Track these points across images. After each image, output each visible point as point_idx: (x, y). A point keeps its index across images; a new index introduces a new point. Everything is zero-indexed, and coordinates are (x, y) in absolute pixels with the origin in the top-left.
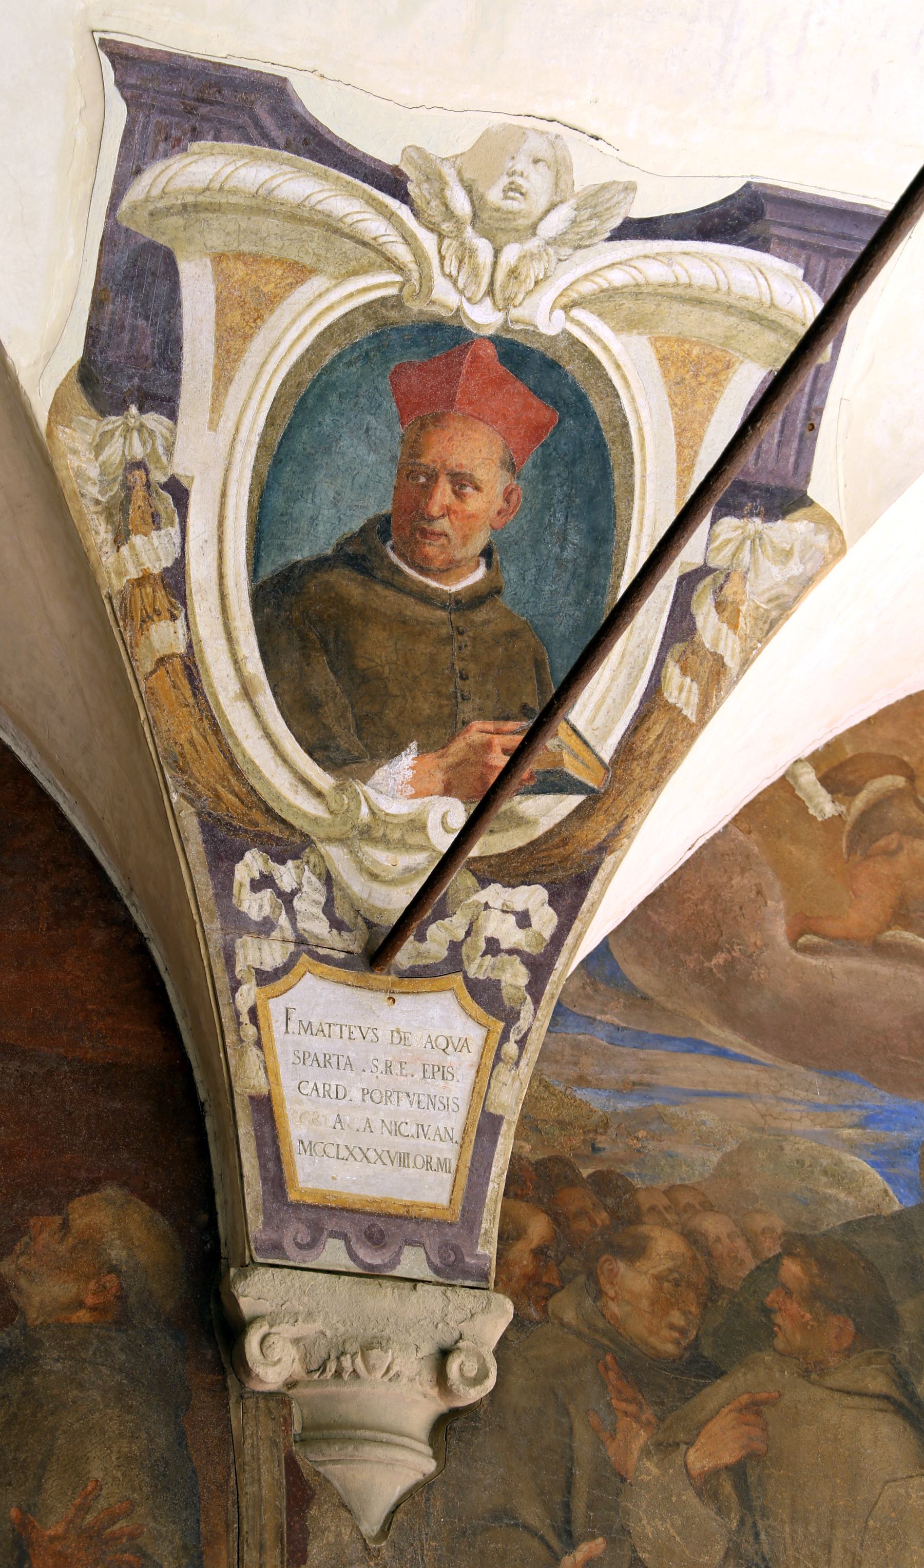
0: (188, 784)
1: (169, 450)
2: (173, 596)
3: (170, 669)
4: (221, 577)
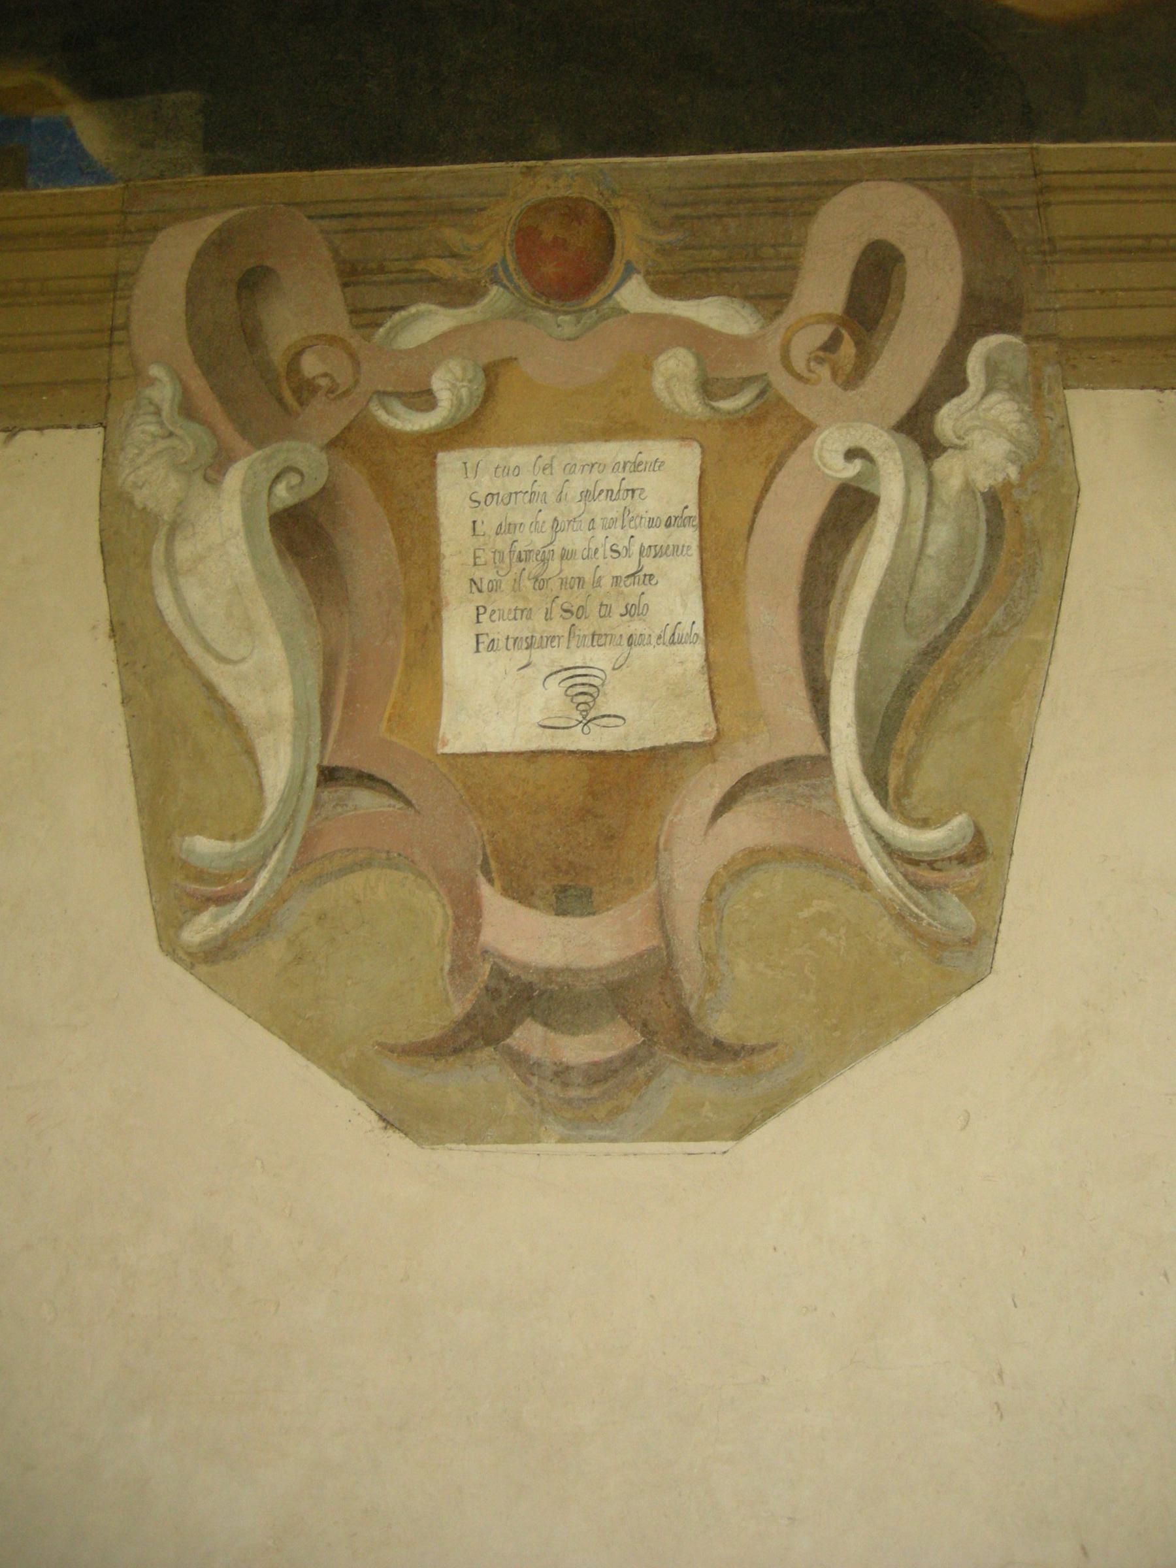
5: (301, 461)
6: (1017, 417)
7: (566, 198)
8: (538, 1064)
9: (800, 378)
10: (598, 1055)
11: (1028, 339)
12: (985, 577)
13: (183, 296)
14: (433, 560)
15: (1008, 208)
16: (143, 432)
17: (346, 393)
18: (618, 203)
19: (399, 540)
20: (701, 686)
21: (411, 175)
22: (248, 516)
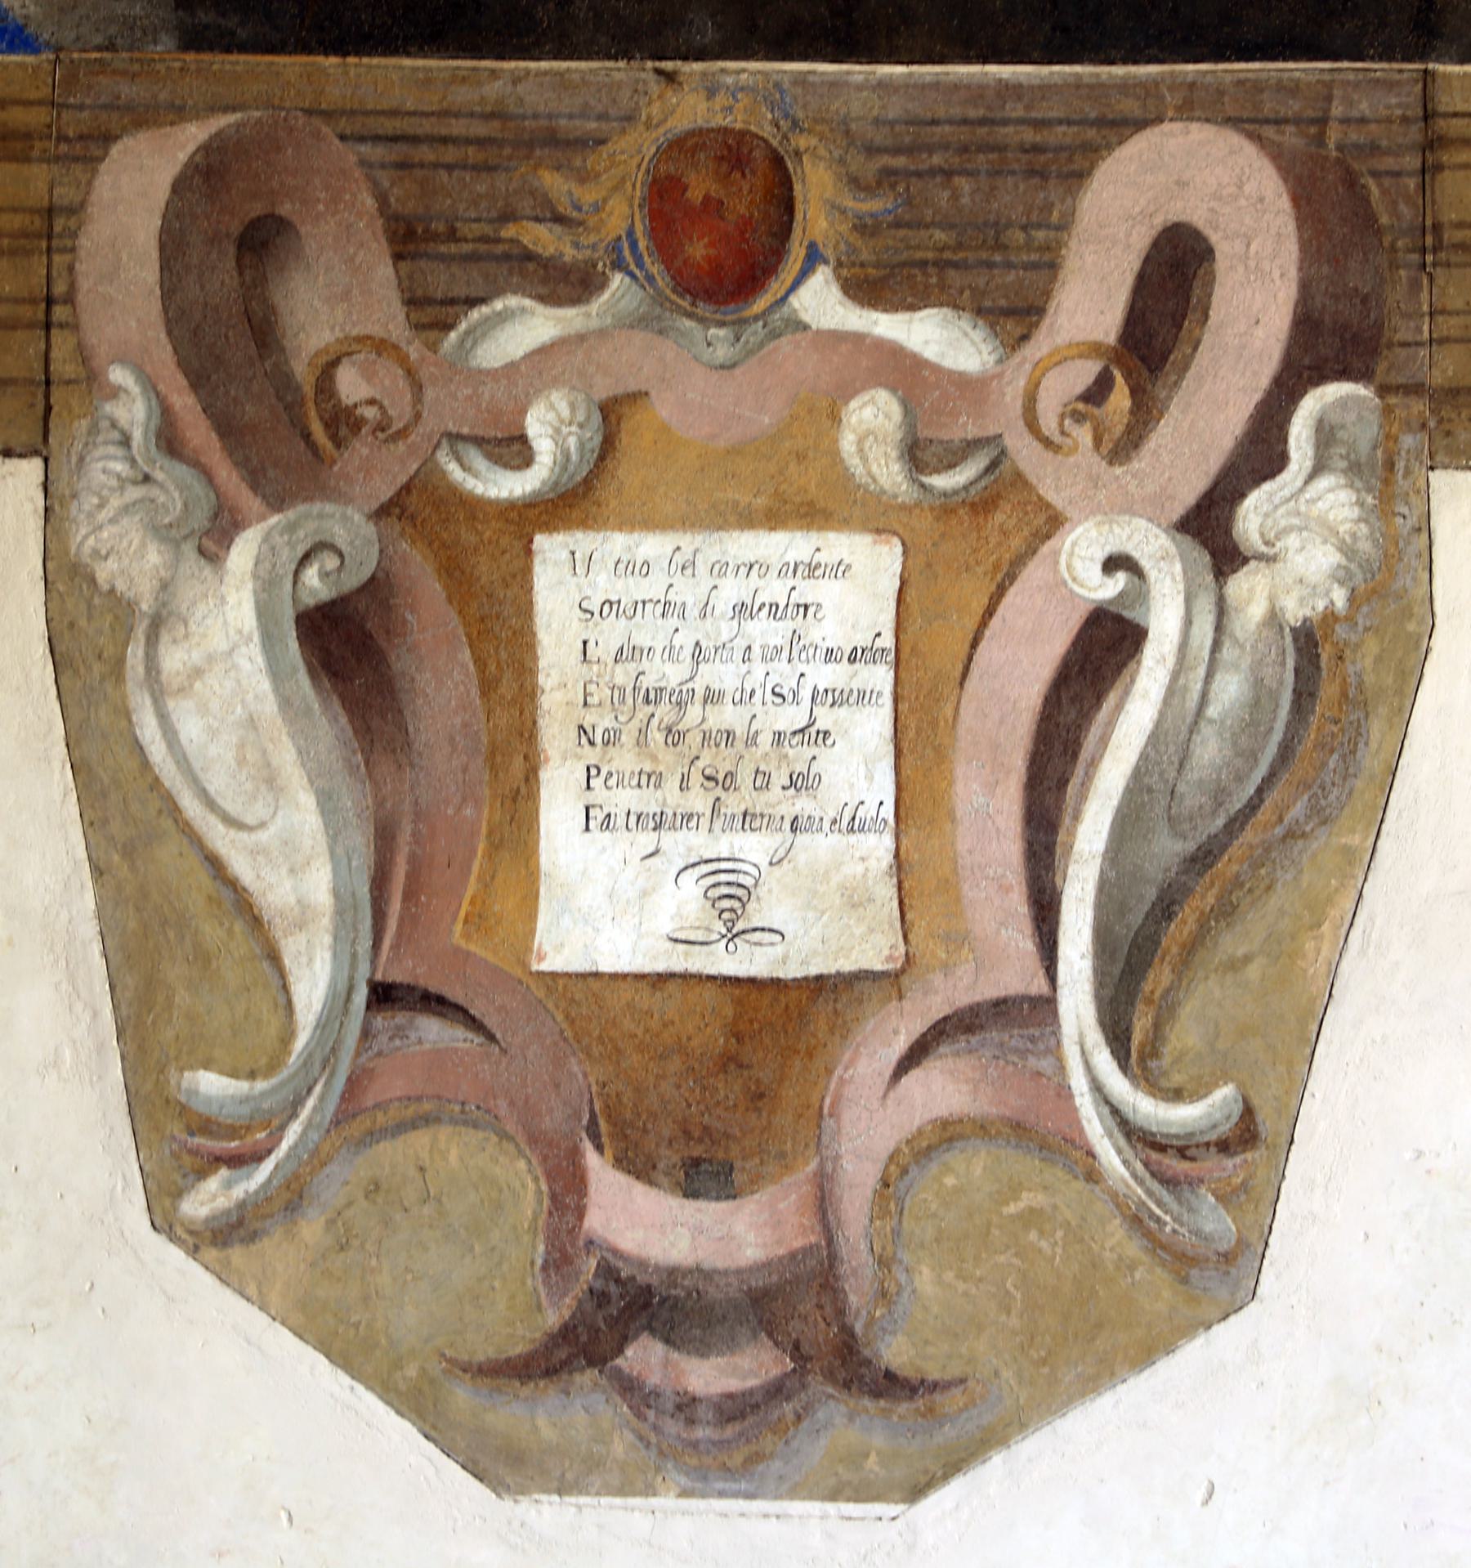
5: (340, 536)
6: (1356, 512)
7: (726, 131)
8: (656, 1394)
9: (1047, 443)
10: (734, 1385)
11: (1383, 391)
13: (155, 254)
14: (527, 695)
15: (1375, 174)
16: (104, 471)
17: (402, 433)
18: (802, 142)
19: (480, 662)
20: (886, 892)
21: (494, 74)
22: (263, 612)
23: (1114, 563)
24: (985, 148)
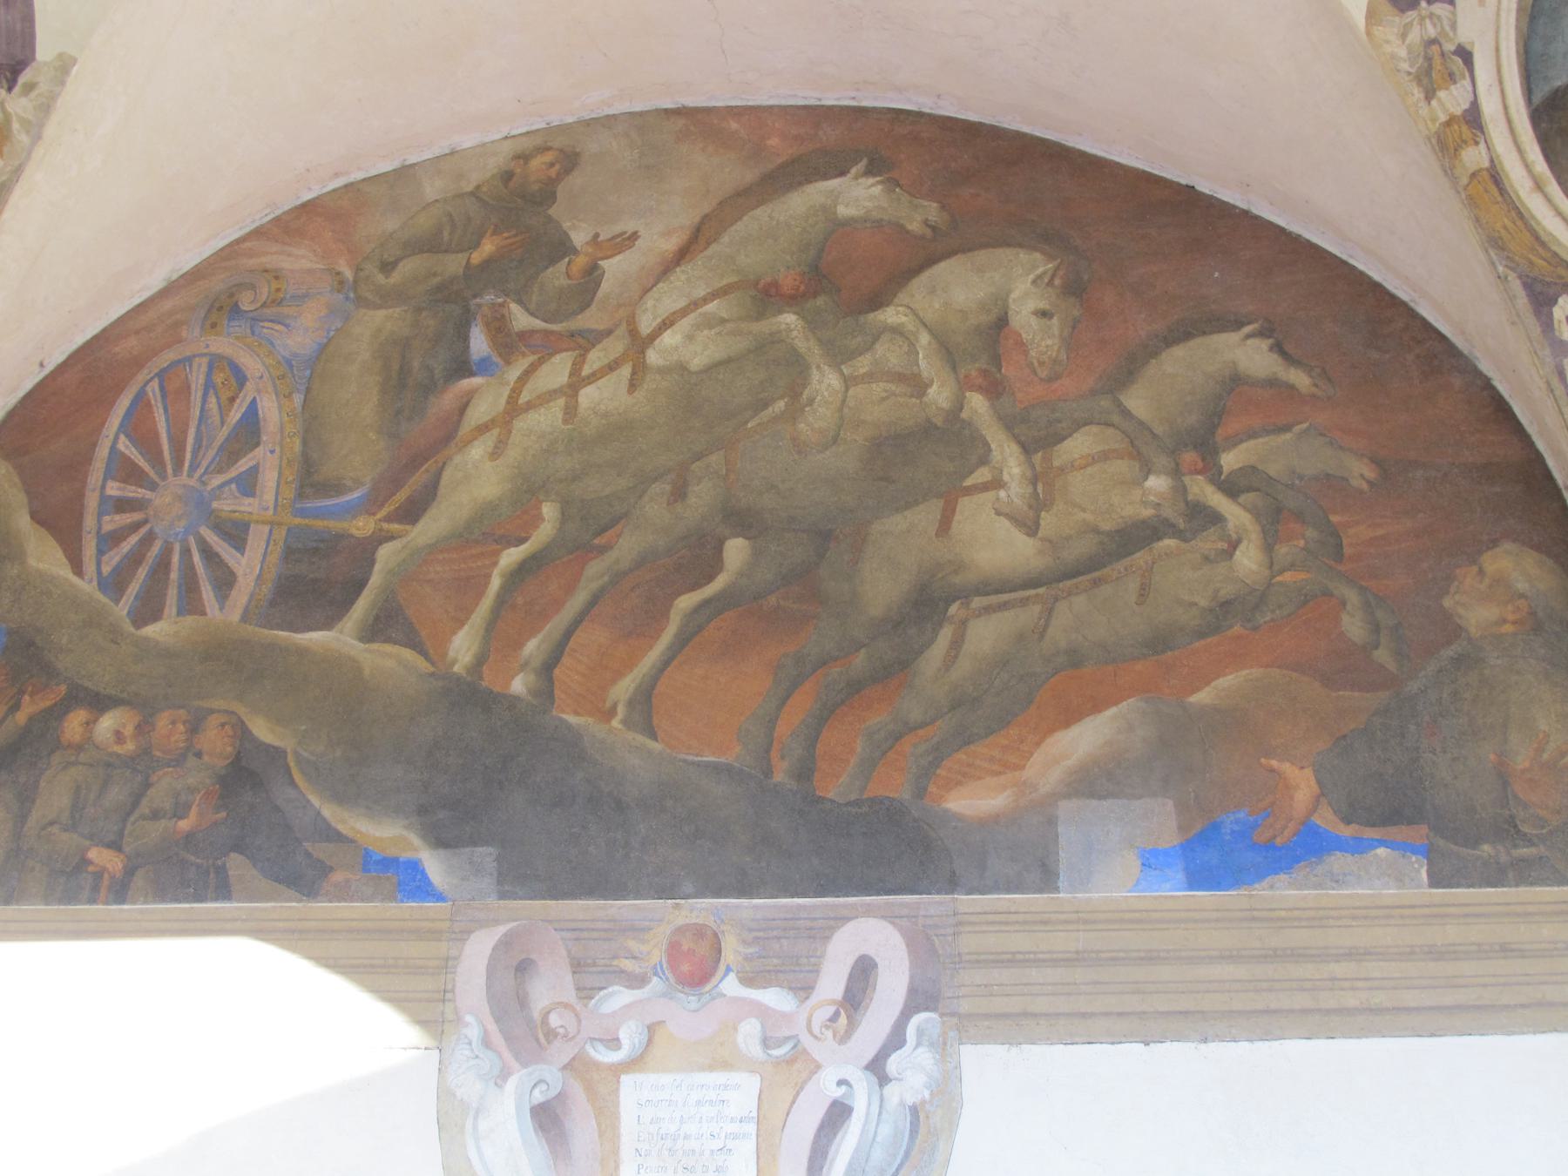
0: (1508, 257)
1: (1454, 26)
2: (1475, 129)
3: (1480, 179)
4: (1506, 108)
6: (932, 1061)
9: (816, 1037)
11: (942, 1015)
12: (907, 1154)
13: (484, 973)
15: (937, 936)
16: (462, 1054)
17: (573, 1037)
18: (723, 927)
19: (599, 1124)
21: (612, 906)
23: (841, 1083)
24: (794, 929)
